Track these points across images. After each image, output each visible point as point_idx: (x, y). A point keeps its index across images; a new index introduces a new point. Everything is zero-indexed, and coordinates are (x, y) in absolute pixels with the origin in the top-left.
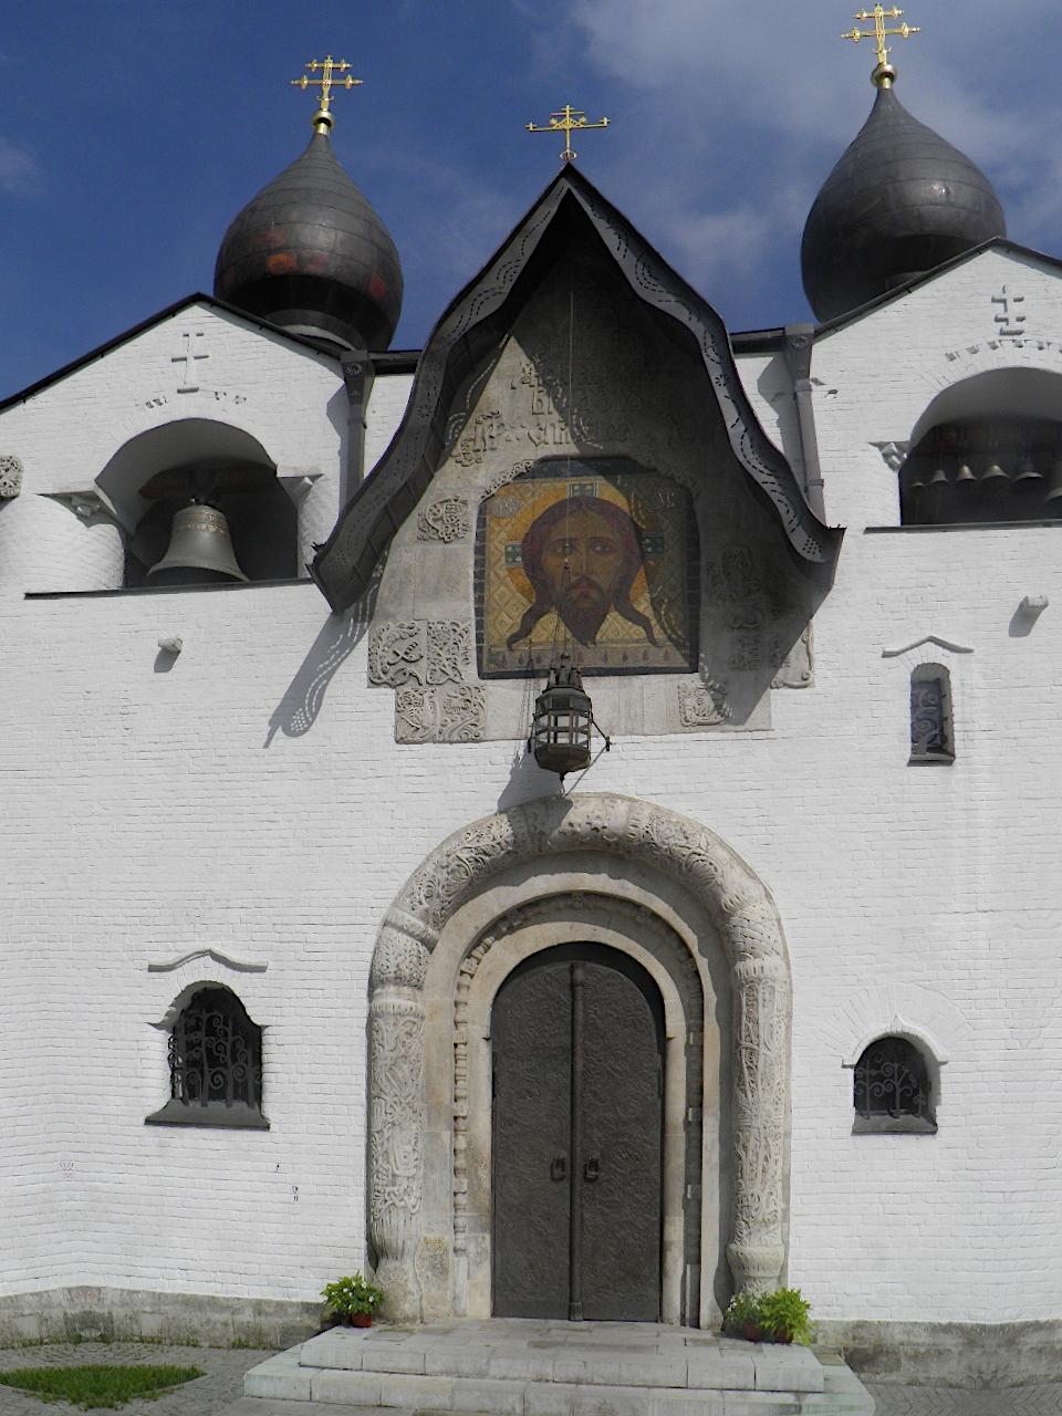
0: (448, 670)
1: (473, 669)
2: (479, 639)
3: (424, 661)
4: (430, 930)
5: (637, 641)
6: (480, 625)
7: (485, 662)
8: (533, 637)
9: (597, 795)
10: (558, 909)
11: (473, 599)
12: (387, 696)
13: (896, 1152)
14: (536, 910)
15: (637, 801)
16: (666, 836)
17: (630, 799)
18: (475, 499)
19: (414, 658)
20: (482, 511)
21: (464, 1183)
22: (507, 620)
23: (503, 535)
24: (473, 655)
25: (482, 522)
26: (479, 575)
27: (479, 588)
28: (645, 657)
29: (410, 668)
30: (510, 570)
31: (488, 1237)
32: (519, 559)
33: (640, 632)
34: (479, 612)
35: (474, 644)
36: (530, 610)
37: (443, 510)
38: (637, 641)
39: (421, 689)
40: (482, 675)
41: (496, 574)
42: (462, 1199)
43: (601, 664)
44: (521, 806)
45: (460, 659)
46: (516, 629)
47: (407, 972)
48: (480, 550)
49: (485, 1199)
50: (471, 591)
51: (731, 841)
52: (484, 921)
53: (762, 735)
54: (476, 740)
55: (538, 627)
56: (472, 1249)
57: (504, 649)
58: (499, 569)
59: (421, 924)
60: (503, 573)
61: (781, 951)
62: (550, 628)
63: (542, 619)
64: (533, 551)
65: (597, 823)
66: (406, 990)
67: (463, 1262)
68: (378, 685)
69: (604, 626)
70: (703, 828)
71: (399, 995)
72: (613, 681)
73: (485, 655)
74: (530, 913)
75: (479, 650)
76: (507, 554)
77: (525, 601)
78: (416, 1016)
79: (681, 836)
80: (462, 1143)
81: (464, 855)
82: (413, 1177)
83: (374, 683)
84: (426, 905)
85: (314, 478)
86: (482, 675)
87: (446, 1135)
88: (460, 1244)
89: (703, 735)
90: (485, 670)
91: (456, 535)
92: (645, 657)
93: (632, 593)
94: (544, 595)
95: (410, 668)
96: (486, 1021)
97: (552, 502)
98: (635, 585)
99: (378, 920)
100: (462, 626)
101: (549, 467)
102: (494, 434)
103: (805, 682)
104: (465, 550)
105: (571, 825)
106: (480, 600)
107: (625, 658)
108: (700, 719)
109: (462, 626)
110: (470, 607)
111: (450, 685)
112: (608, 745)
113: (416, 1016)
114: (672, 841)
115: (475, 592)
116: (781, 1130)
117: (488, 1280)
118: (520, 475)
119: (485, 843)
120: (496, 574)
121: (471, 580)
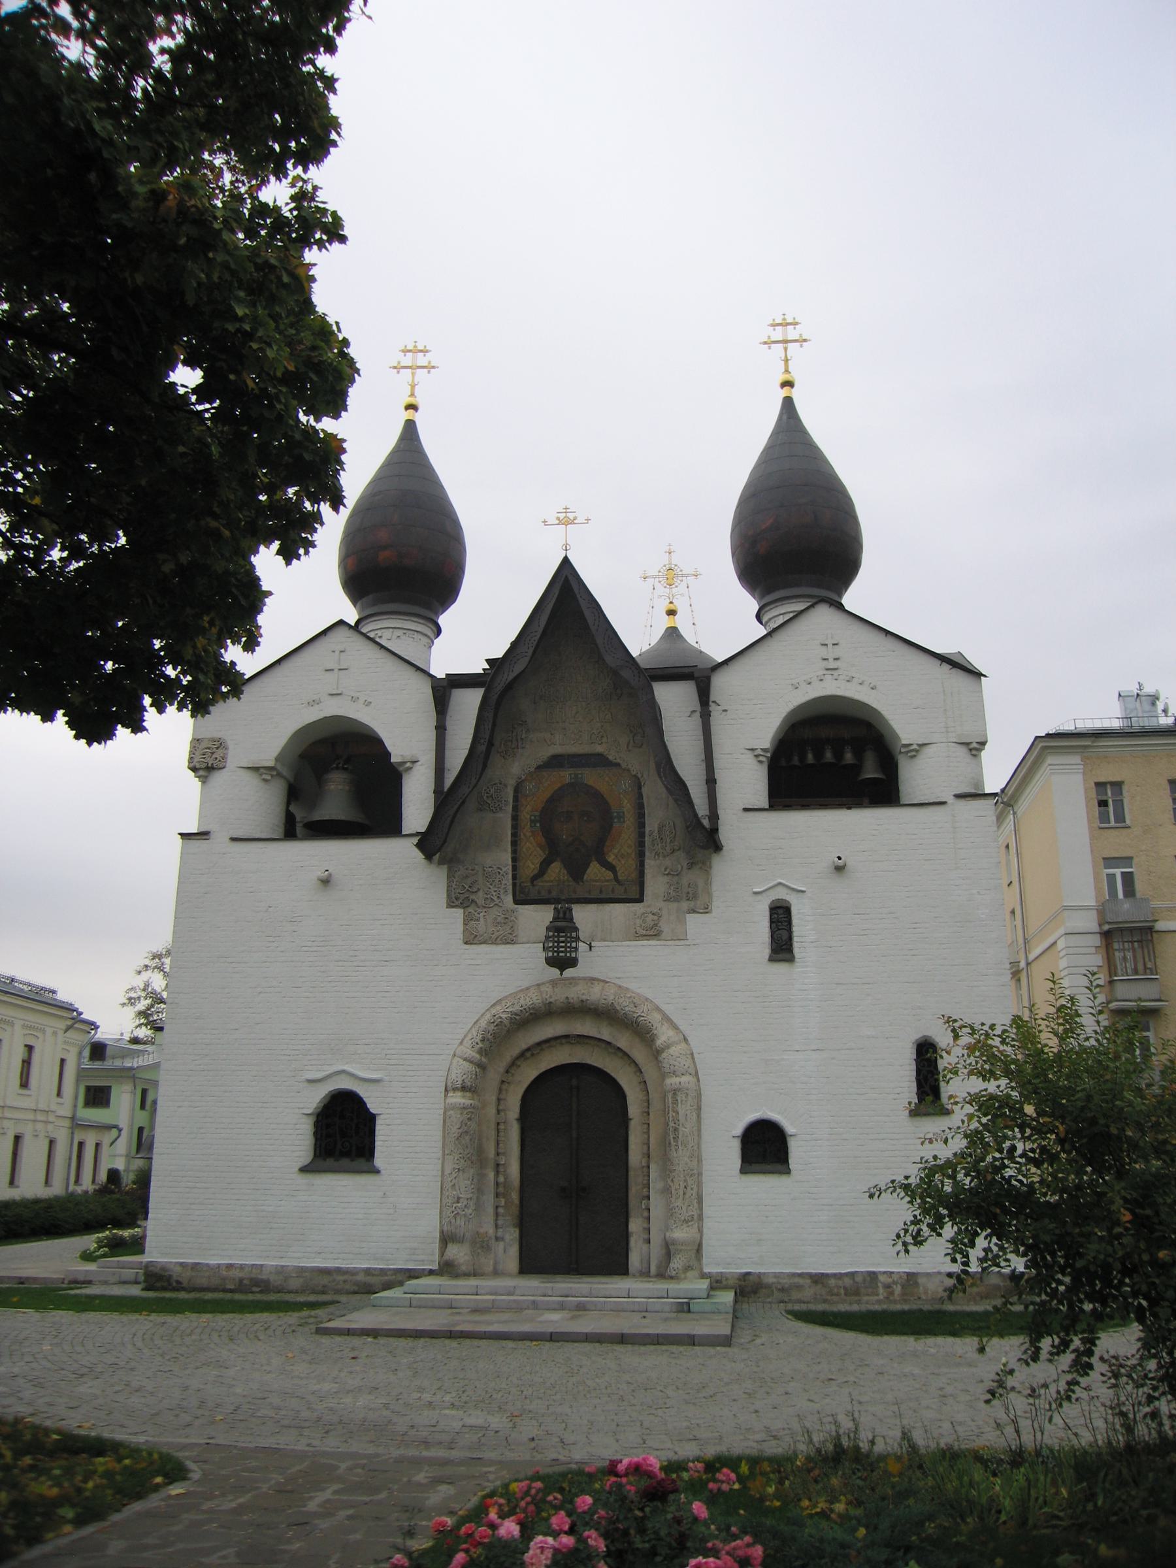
0: (495, 898)
1: (510, 898)
2: (514, 877)
3: (481, 894)
4: (483, 1059)
5: (608, 881)
6: (514, 868)
7: (517, 893)
8: (546, 877)
9: (584, 979)
10: (562, 1044)
11: (510, 850)
12: (459, 913)
13: (764, 1185)
14: (548, 1045)
15: (607, 982)
16: (624, 1005)
17: (603, 981)
18: (512, 782)
19: (475, 890)
20: (517, 790)
21: (502, 1202)
22: (531, 866)
23: (529, 808)
24: (510, 888)
25: (516, 799)
26: (514, 835)
27: (514, 843)
28: (613, 891)
29: (472, 897)
30: (532, 832)
31: (517, 1231)
32: (538, 825)
33: (609, 875)
34: (514, 860)
35: (511, 881)
36: (545, 859)
37: (493, 791)
38: (608, 881)
39: (479, 910)
40: (517, 902)
41: (525, 835)
42: (501, 1210)
43: (587, 896)
44: (538, 985)
45: (502, 891)
46: (536, 872)
47: (469, 1084)
48: (515, 818)
49: (515, 1210)
50: (510, 846)
51: (664, 1007)
52: (516, 1051)
53: (682, 942)
54: (512, 942)
55: (549, 871)
56: (508, 1237)
57: (529, 884)
58: (526, 831)
59: (478, 1056)
60: (528, 834)
61: (692, 1071)
62: (556, 870)
63: (553, 865)
64: (547, 818)
65: (584, 997)
66: (468, 1094)
67: (501, 1245)
68: (453, 907)
69: (589, 871)
70: (647, 999)
71: (464, 1097)
72: (592, 907)
73: (518, 888)
74: (544, 1046)
75: (514, 885)
76: (532, 821)
77: (541, 852)
78: (474, 1108)
79: (632, 1005)
80: (501, 1179)
81: (504, 1016)
82: (471, 1199)
83: (450, 905)
84: (480, 1045)
85: (414, 762)
86: (517, 902)
87: (491, 1175)
88: (499, 1234)
89: (645, 942)
90: (518, 898)
91: (500, 809)
92: (613, 891)
93: (605, 849)
94: (553, 850)
95: (472, 897)
96: (517, 1110)
97: (559, 785)
98: (607, 843)
99: (452, 1053)
100: (504, 869)
101: (556, 762)
102: (523, 736)
103: (707, 910)
104: (505, 818)
105: (567, 998)
106: (514, 852)
107: (601, 892)
108: (644, 932)
109: (504, 869)
110: (507, 857)
111: (496, 908)
112: (591, 947)
113: (474, 1108)
114: (627, 1009)
115: (512, 845)
116: (695, 1171)
117: (518, 1254)
118: (539, 768)
119: (517, 1008)
120: (525, 835)
121: (509, 838)
